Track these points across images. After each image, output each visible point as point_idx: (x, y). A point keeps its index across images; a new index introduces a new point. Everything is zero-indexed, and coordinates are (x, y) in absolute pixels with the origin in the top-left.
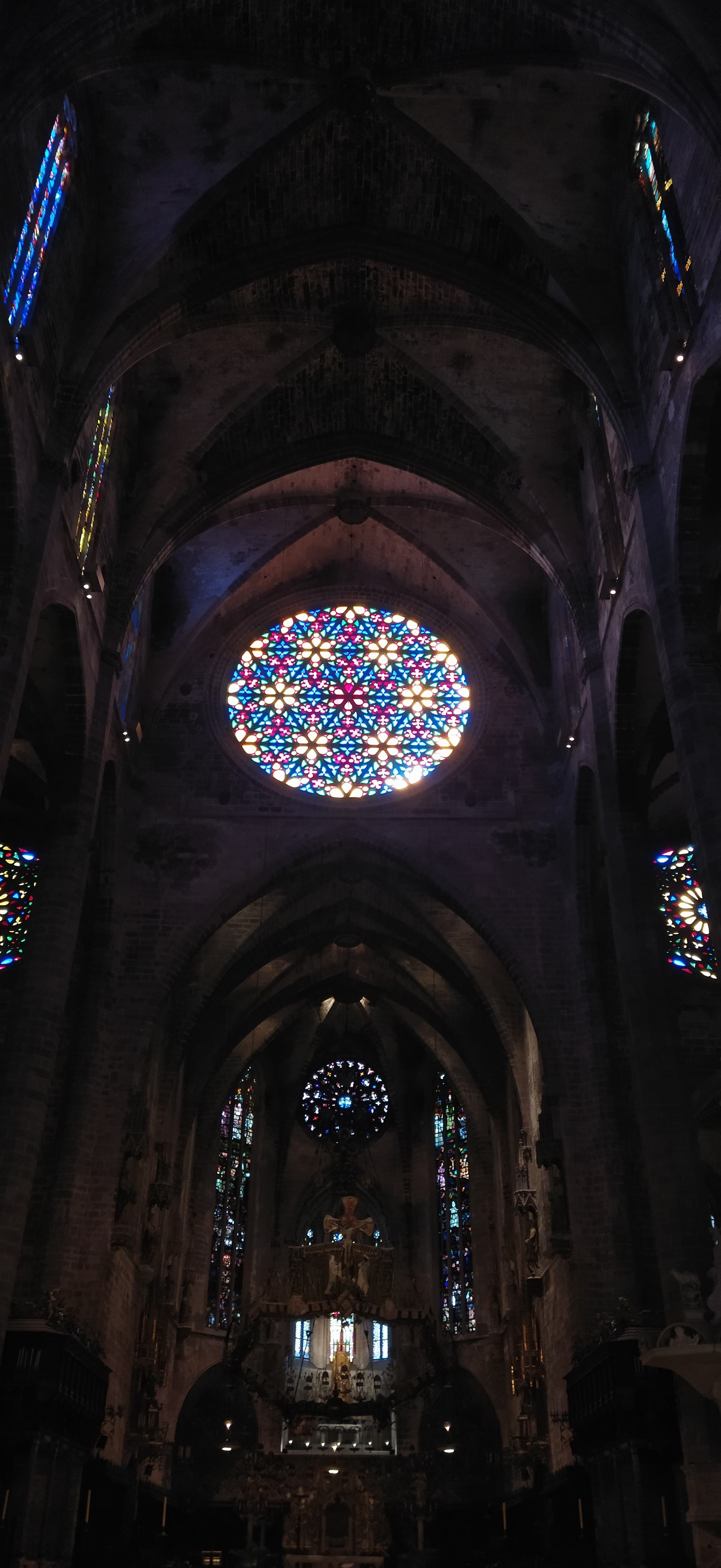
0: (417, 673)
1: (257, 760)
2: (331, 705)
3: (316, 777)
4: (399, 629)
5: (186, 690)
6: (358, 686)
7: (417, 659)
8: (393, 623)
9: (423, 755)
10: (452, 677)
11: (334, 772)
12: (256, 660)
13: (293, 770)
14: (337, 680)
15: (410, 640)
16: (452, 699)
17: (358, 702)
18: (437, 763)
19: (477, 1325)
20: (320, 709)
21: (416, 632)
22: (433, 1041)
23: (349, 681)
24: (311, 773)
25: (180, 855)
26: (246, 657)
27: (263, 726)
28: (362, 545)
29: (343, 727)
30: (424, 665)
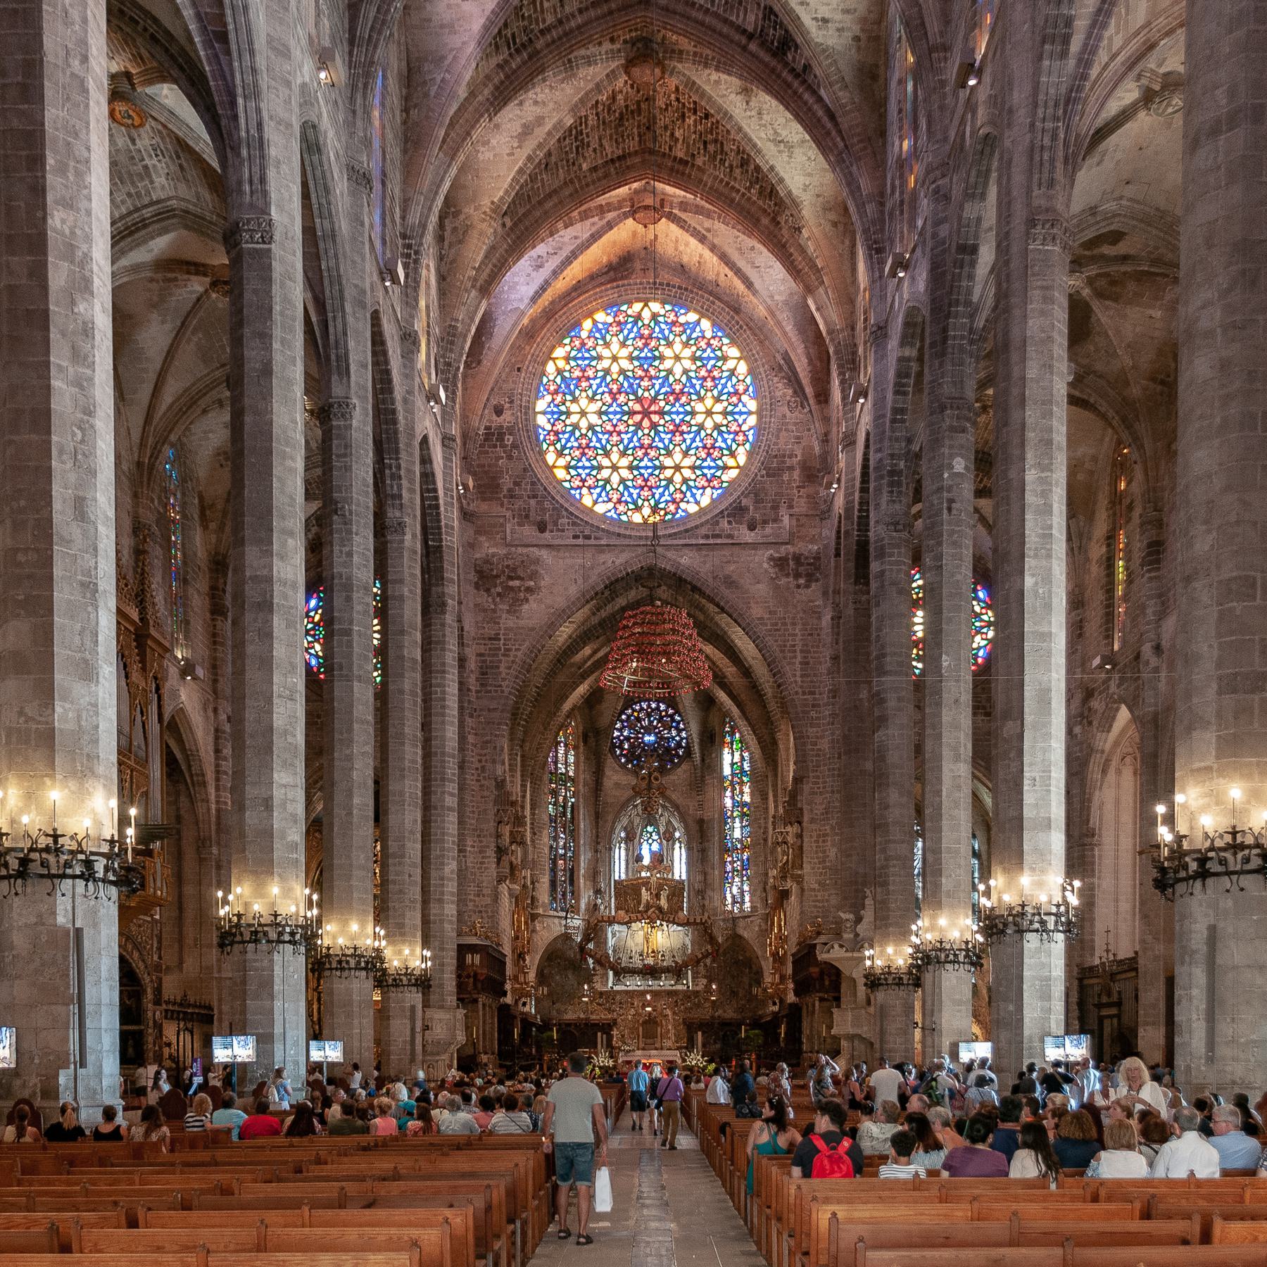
0: (709, 384)
1: (567, 485)
2: (630, 422)
3: (619, 501)
4: (693, 330)
5: (499, 411)
6: (654, 400)
7: (709, 367)
8: (688, 323)
9: (713, 476)
10: (741, 388)
11: (635, 496)
12: (559, 372)
13: (599, 495)
14: (635, 393)
15: (703, 344)
16: (741, 413)
17: (655, 418)
18: (725, 485)
20: (622, 427)
21: (708, 334)
23: (646, 394)
24: (615, 497)
25: (511, 583)
26: (550, 368)
27: (571, 448)
28: (656, 236)
29: (642, 447)
30: (716, 373)
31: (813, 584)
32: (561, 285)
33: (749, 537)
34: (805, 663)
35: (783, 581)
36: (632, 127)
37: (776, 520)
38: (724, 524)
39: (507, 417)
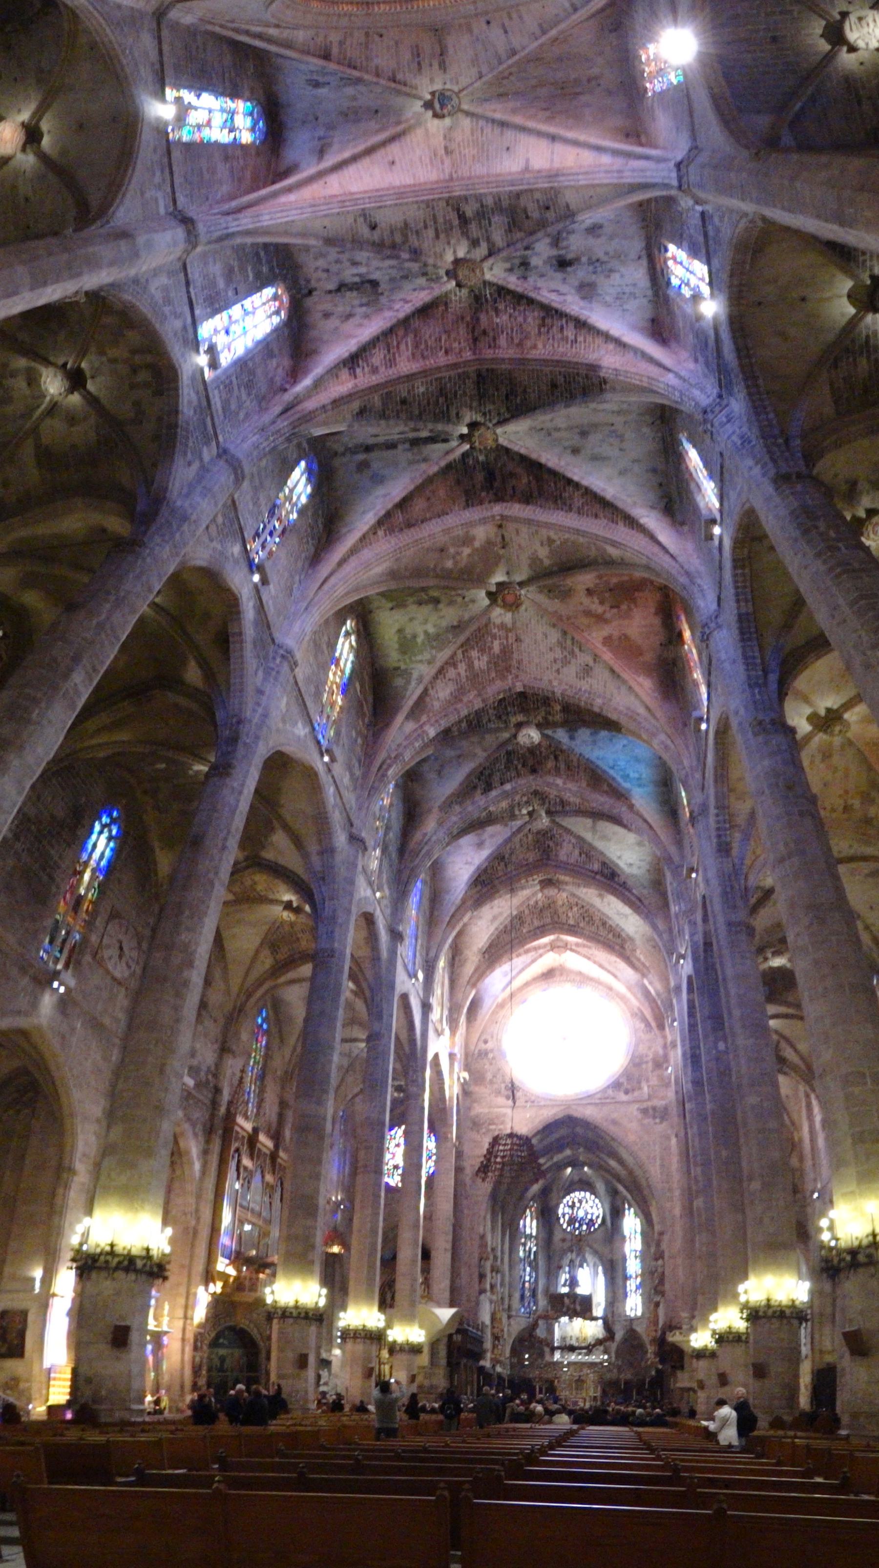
5: (486, 1042)
19: (643, 1314)
22: (621, 1188)
31: (665, 1124)
32: (517, 983)
33: (623, 1097)
34: (662, 1166)
35: (646, 1121)
36: (547, 913)
37: (640, 1088)
38: (610, 1092)
39: (490, 1045)
